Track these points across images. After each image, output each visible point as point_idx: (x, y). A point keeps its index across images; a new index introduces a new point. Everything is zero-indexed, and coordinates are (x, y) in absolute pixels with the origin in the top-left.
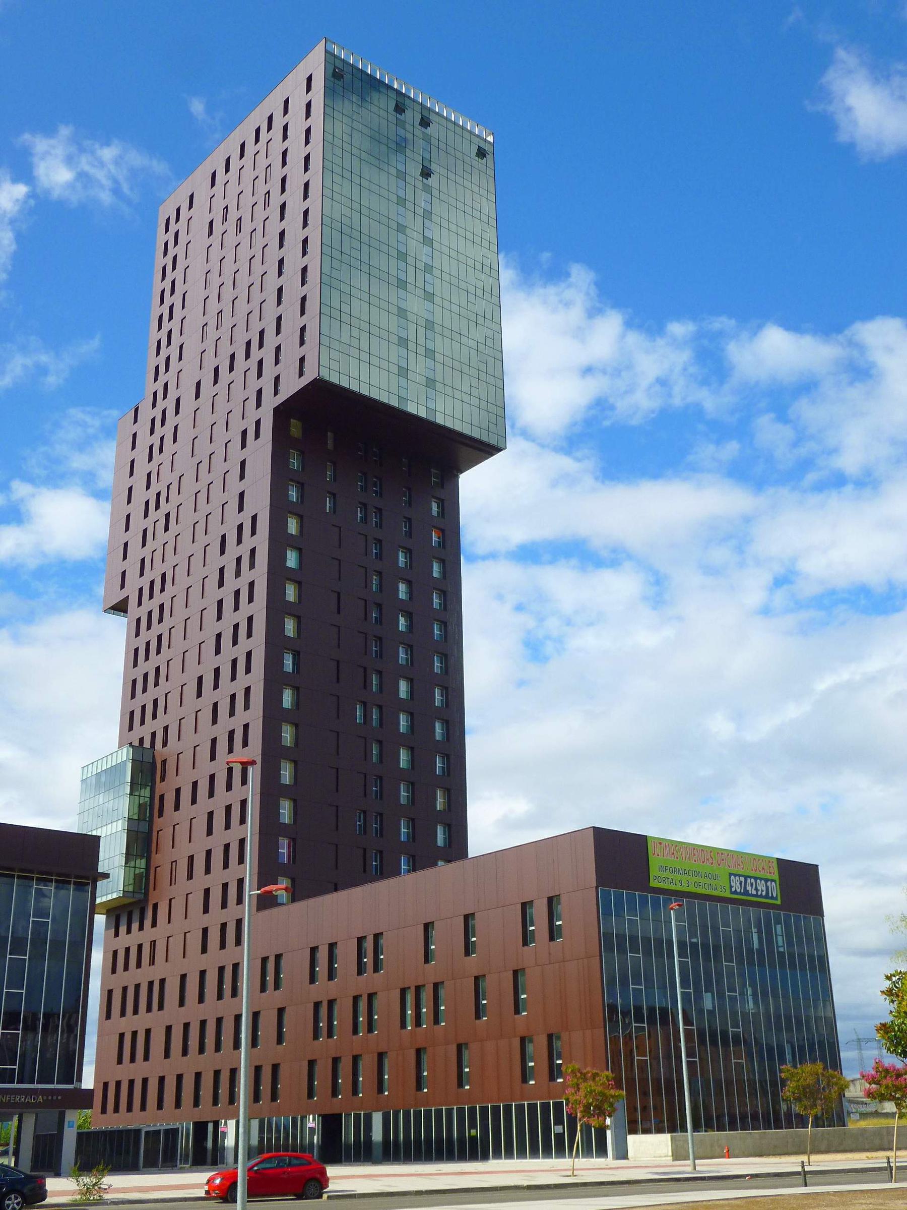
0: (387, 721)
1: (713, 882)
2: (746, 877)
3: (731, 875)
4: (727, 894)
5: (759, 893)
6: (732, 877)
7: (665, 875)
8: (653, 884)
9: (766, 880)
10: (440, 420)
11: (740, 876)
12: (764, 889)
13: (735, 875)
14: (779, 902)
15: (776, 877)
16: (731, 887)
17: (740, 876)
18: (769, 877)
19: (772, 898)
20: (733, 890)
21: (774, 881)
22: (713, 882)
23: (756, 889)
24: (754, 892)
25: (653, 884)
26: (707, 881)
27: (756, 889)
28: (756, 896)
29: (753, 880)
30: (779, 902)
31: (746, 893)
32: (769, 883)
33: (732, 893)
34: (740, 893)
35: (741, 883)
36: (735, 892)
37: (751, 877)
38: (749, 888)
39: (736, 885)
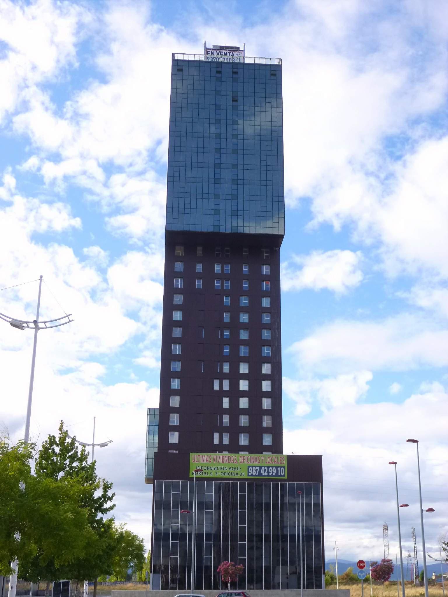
0: (234, 385)
1: (235, 472)
2: (261, 467)
3: (249, 467)
4: (246, 476)
5: (270, 474)
9: (277, 467)
11: (256, 467)
12: (275, 472)
13: (252, 467)
14: (286, 477)
15: (285, 465)
16: (249, 472)
17: (256, 467)
18: (279, 465)
19: (281, 476)
20: (250, 474)
22: (235, 472)
23: (268, 472)
24: (266, 474)
26: (232, 471)
27: (268, 472)
28: (268, 475)
29: (266, 468)
30: (286, 477)
31: (260, 474)
32: (279, 469)
33: (249, 475)
34: (256, 475)
35: (256, 470)
36: (252, 475)
37: (264, 467)
38: (262, 472)
39: (253, 471)
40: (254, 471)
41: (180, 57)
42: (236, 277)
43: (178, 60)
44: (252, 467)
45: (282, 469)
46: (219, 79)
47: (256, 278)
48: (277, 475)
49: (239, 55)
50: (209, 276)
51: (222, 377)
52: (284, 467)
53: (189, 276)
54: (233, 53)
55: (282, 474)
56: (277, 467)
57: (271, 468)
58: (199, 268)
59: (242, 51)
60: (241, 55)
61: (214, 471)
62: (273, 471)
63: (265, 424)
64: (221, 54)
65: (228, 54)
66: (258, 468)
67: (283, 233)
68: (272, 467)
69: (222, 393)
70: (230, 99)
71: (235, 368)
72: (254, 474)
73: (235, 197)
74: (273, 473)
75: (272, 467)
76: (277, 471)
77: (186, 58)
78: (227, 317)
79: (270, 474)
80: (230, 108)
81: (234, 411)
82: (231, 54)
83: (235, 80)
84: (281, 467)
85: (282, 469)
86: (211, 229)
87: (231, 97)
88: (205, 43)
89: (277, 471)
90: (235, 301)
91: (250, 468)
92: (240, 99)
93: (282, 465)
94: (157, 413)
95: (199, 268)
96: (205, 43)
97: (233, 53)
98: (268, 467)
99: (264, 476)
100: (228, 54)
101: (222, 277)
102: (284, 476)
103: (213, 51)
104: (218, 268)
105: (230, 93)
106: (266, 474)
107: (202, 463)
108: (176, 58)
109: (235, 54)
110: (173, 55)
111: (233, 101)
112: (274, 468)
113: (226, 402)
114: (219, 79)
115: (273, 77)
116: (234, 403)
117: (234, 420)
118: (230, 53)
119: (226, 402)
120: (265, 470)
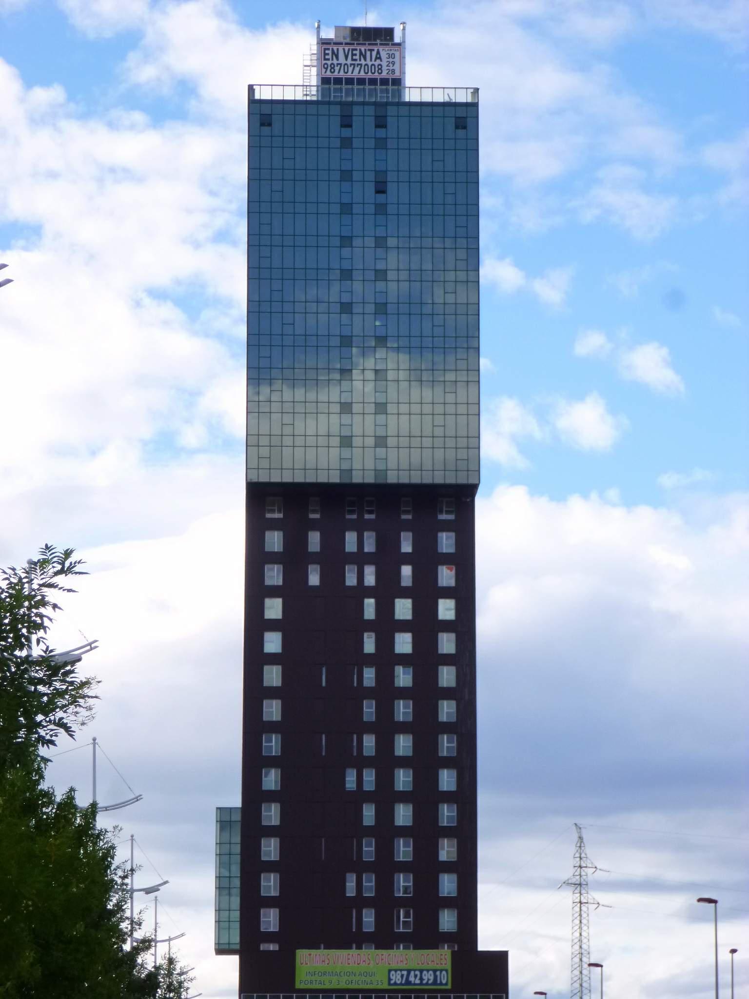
0: (385, 780)
1: (368, 979)
2: (409, 971)
4: (385, 986)
5: (424, 982)
6: (393, 972)
7: (313, 978)
8: (299, 985)
9: (435, 971)
11: (401, 970)
12: (432, 978)
14: (449, 987)
16: (390, 979)
17: (401, 970)
18: (438, 967)
19: (441, 984)
20: (392, 982)
21: (446, 971)
22: (368, 979)
23: (421, 979)
24: (418, 981)
25: (299, 985)
26: (363, 978)
27: (421, 979)
28: (421, 984)
29: (418, 973)
30: (449, 987)
31: (408, 982)
33: (390, 984)
34: (401, 984)
35: (402, 976)
36: (395, 984)
37: (415, 970)
38: (412, 979)
39: (396, 978)
40: (399, 977)
42: (387, 559)
44: (396, 971)
45: (444, 972)
46: (347, 143)
47: (426, 560)
48: (435, 982)
49: (391, 56)
50: (334, 560)
51: (361, 763)
52: (446, 971)
53: (294, 558)
54: (378, 52)
55: (444, 982)
56: (435, 971)
57: (425, 972)
58: (314, 540)
59: (399, 44)
60: (397, 54)
61: (335, 979)
62: (428, 977)
63: (443, 856)
64: (353, 55)
65: (368, 53)
66: (405, 973)
67: (477, 482)
68: (428, 971)
69: (361, 796)
70: (370, 188)
71: (385, 744)
72: (399, 982)
73: (381, 408)
74: (429, 980)
75: (428, 971)
76: (435, 977)
77: (277, 95)
78: (369, 645)
79: (424, 982)
80: (371, 209)
81: (386, 831)
82: (374, 54)
83: (381, 144)
84: (441, 971)
85: (444, 972)
86: (335, 479)
89: (435, 977)
90: (385, 608)
91: (393, 972)
92: (391, 188)
93: (443, 967)
94: (237, 817)
95: (314, 540)
97: (378, 52)
98: (421, 971)
99: (415, 984)
100: (368, 53)
101: (360, 559)
102: (446, 984)
103: (335, 48)
104: (351, 540)
105: (370, 176)
106: (418, 981)
107: (315, 966)
108: (257, 97)
109: (383, 54)
110: (251, 89)
111: (378, 192)
112: (431, 972)
113: (369, 814)
114: (347, 143)
115: (461, 133)
116: (385, 815)
117: (385, 849)
118: (371, 50)
119: (369, 814)
120: (416, 976)
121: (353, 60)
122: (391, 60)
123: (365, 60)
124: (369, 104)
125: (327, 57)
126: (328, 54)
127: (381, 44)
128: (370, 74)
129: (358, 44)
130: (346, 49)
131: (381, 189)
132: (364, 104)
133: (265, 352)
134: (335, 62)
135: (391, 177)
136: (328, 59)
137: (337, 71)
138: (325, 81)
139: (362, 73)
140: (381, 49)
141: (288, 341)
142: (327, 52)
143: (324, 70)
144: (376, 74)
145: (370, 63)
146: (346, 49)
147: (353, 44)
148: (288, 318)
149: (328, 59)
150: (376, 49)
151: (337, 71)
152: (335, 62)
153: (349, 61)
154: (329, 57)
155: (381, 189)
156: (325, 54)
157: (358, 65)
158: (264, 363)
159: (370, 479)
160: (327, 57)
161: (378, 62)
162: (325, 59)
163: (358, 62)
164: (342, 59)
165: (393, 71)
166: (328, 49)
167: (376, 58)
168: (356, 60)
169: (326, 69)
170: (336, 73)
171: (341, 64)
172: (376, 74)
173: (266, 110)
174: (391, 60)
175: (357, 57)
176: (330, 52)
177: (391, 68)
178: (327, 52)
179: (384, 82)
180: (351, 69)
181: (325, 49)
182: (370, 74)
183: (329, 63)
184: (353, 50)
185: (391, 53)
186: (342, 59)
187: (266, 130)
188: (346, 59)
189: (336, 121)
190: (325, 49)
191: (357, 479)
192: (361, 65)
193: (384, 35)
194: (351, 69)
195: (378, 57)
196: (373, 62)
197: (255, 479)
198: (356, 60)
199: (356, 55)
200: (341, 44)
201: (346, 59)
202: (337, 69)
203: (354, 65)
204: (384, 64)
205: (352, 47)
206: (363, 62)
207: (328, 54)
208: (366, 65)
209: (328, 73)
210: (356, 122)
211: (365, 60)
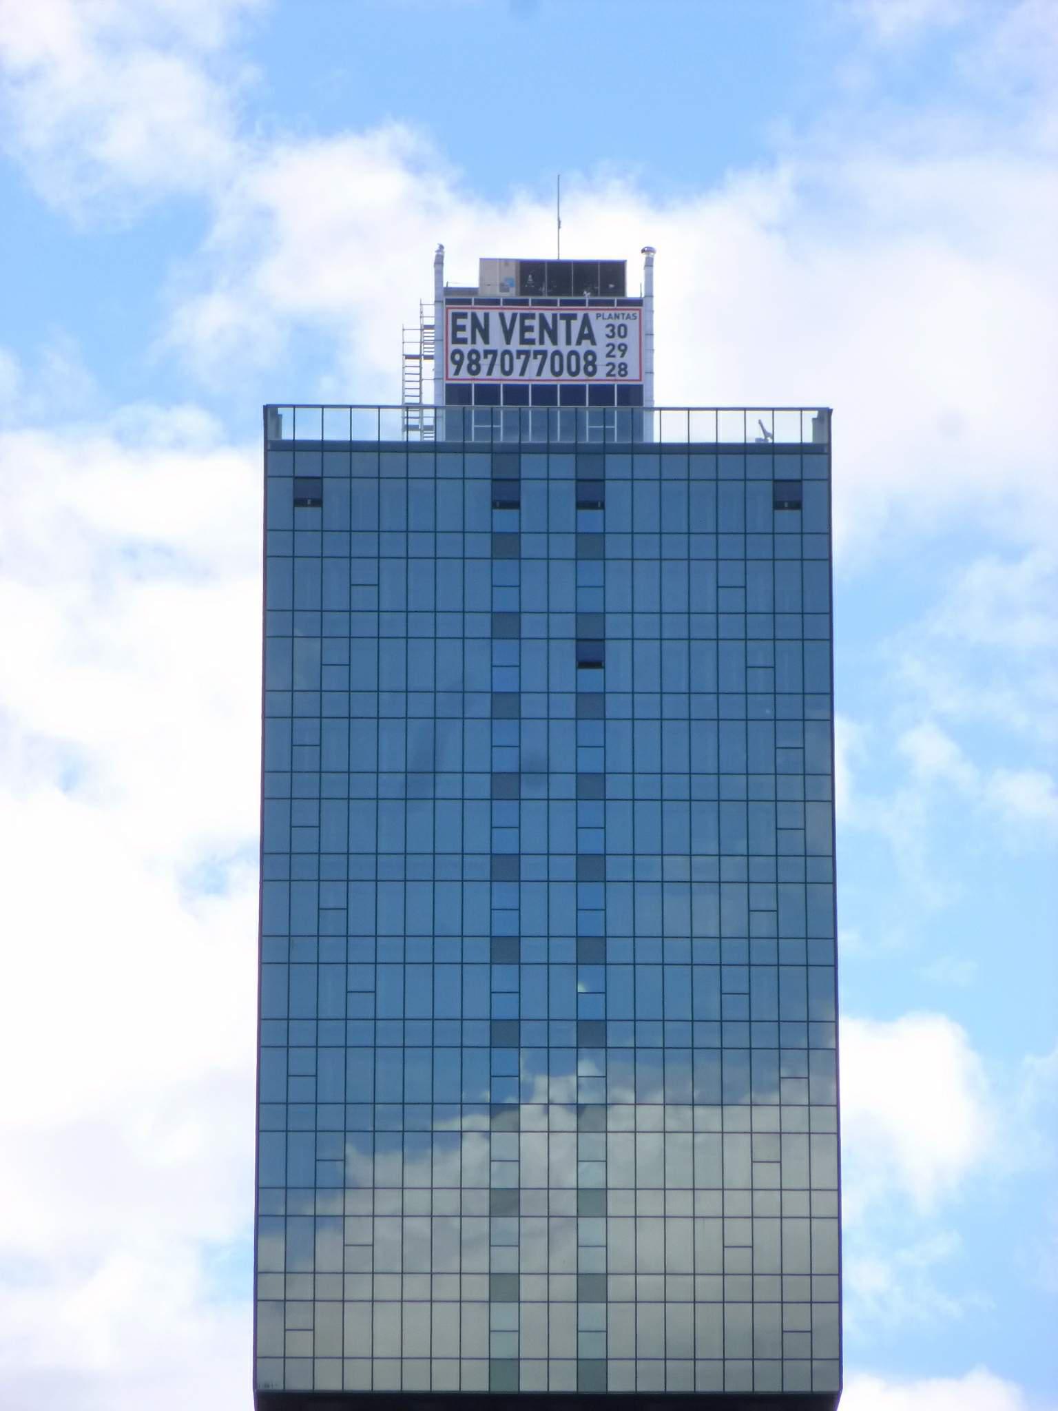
10: (620, 1382)
41: (305, 429)
43: (295, 447)
46: (506, 546)
49: (618, 331)
54: (586, 322)
59: (638, 303)
60: (632, 326)
64: (524, 329)
65: (562, 324)
67: (836, 1389)
70: (566, 654)
73: (593, 1201)
80: (566, 706)
82: (576, 325)
83: (591, 547)
86: (476, 1381)
87: (570, 646)
88: (439, 262)
92: (616, 654)
96: (439, 262)
100: (562, 324)
103: (480, 315)
105: (565, 626)
108: (286, 435)
109: (599, 328)
110: (271, 414)
111: (582, 664)
114: (506, 546)
115: (787, 518)
118: (569, 318)
121: (523, 341)
122: (617, 341)
123: (555, 342)
124: (562, 450)
125: (460, 335)
126: (463, 328)
127: (592, 303)
128: (565, 375)
129: (535, 303)
130: (508, 315)
131: (590, 660)
132: (548, 450)
133: (303, 1061)
134: (480, 346)
135: (615, 626)
136: (464, 341)
137: (485, 369)
138: (455, 394)
139: (547, 374)
140: (592, 315)
141: (361, 1033)
142: (460, 322)
143: (452, 368)
144: (582, 375)
145: (565, 350)
146: (508, 315)
147: (525, 303)
148: (361, 978)
149: (464, 341)
150: (580, 314)
151: (485, 369)
152: (480, 346)
153: (515, 345)
154: (467, 334)
155: (590, 660)
156: (457, 328)
157: (536, 353)
158: (302, 1090)
159: (564, 1382)
160: (460, 335)
161: (586, 345)
162: (456, 341)
163: (537, 347)
164: (497, 340)
165: (623, 368)
166: (464, 316)
167: (582, 337)
168: (532, 342)
169: (459, 364)
170: (483, 374)
171: (494, 353)
172: (582, 375)
173: (308, 466)
174: (617, 341)
175: (535, 335)
176: (467, 322)
177: (617, 360)
178: (460, 322)
179: (602, 394)
180: (518, 364)
181: (456, 316)
182: (565, 375)
183: (466, 348)
184: (524, 317)
185: (617, 323)
186: (497, 340)
187: (308, 515)
188: (508, 341)
189: (481, 491)
190: (456, 316)
191: (531, 1382)
192: (544, 353)
193: (599, 281)
194: (518, 364)
195: (587, 334)
196: (573, 347)
197: (277, 1385)
198: (532, 342)
199: (531, 329)
200: (496, 302)
201: (508, 341)
202: (485, 363)
203: (527, 353)
204: (601, 349)
205: (520, 310)
206: (549, 346)
207: (463, 328)
208: (557, 353)
209: (464, 373)
210: (530, 493)
211: (555, 342)
